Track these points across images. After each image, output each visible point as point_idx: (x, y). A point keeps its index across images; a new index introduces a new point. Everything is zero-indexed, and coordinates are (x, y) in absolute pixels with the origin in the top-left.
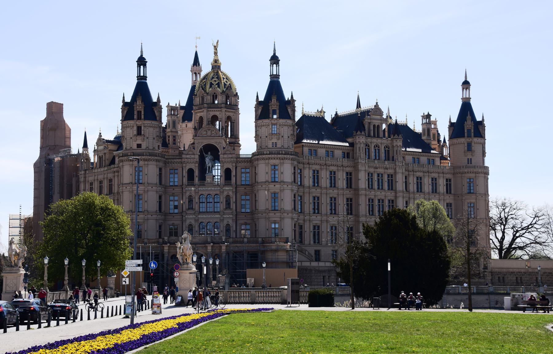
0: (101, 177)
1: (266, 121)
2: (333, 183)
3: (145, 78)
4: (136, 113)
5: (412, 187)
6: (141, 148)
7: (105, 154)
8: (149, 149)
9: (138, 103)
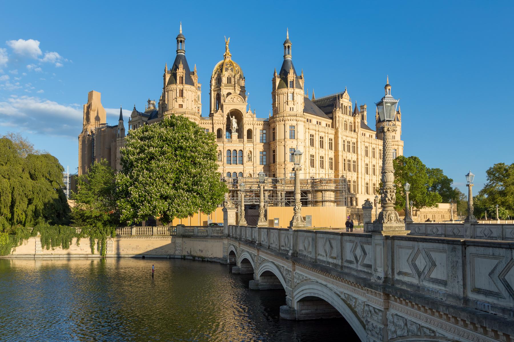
2: (322, 146)
5: (363, 153)
6: (182, 107)
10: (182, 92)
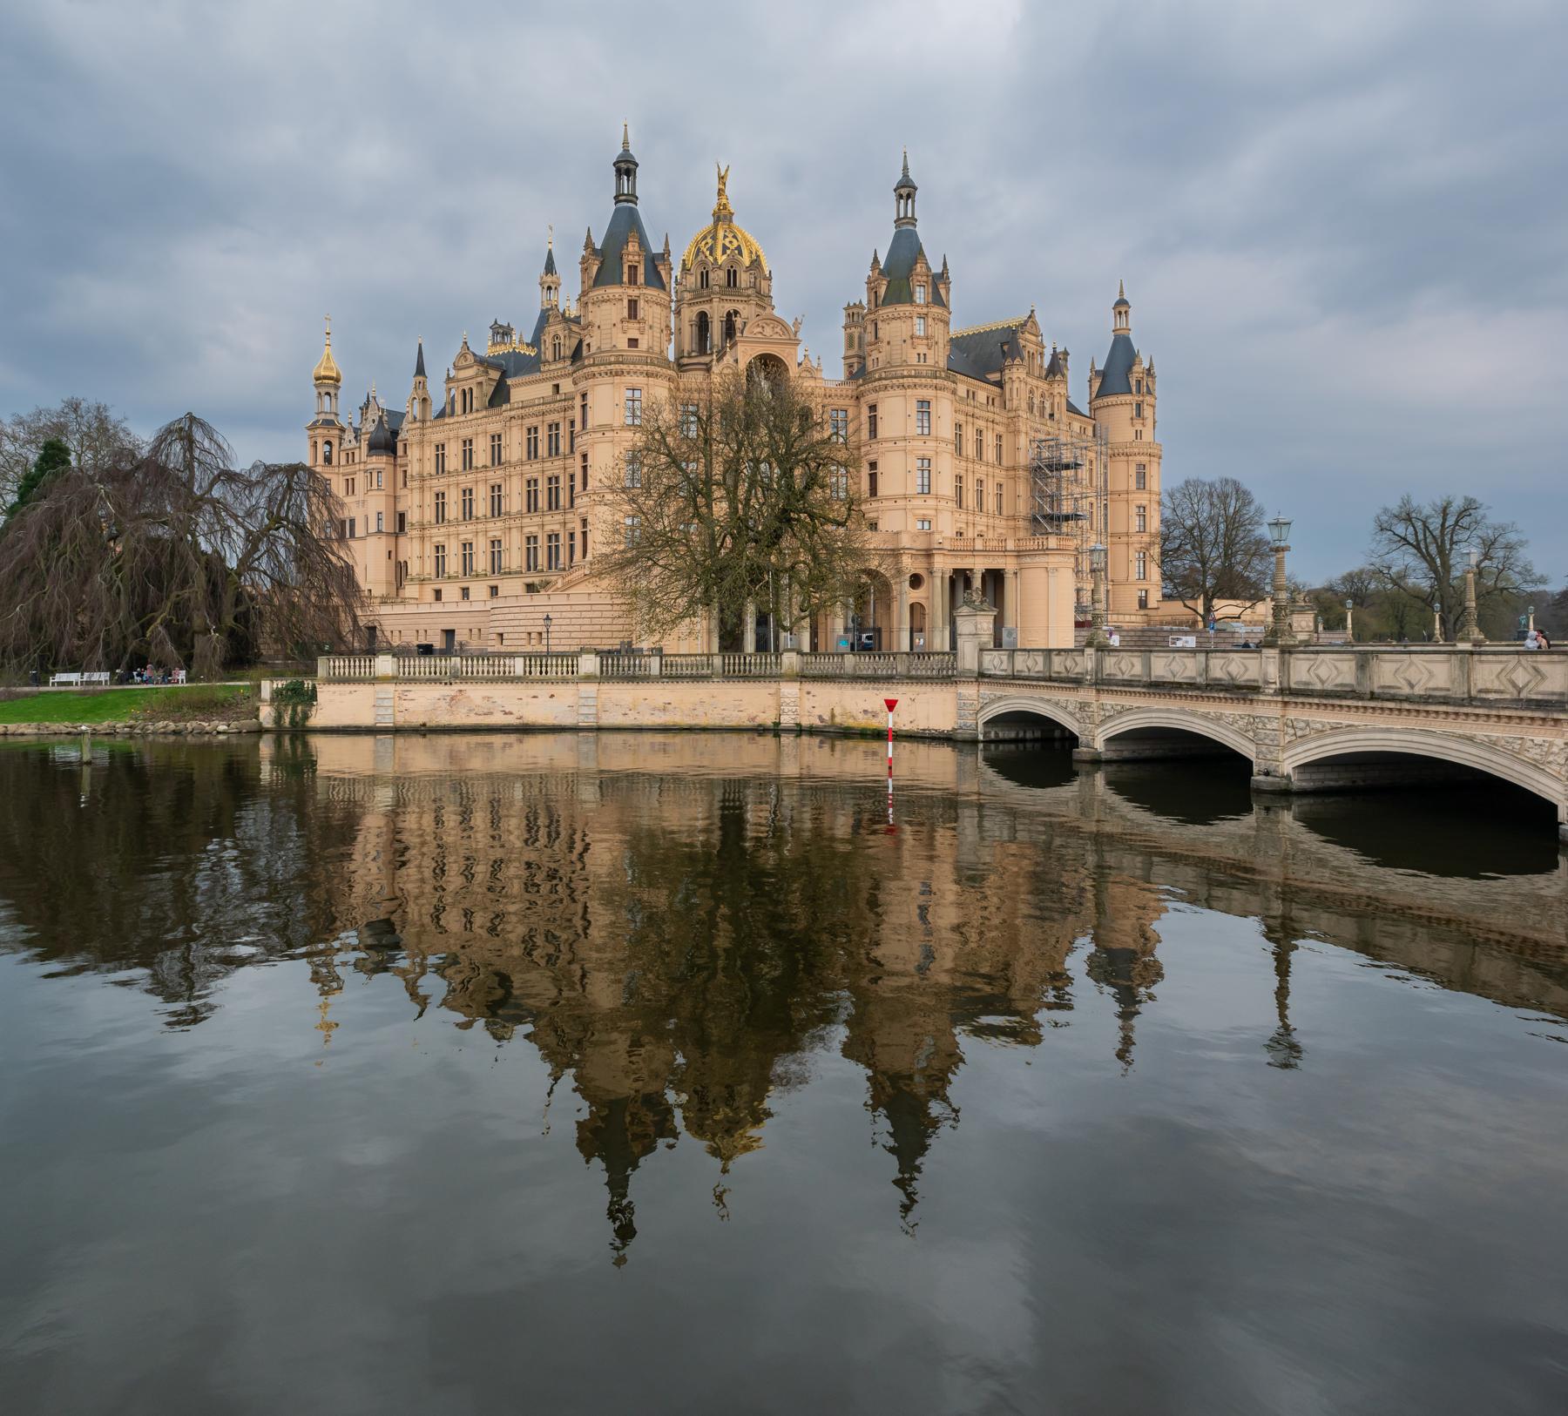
0: (466, 432)
1: (904, 309)
3: (632, 198)
4: (626, 269)
7: (480, 384)
8: (653, 353)
9: (630, 248)
10: (633, 304)
